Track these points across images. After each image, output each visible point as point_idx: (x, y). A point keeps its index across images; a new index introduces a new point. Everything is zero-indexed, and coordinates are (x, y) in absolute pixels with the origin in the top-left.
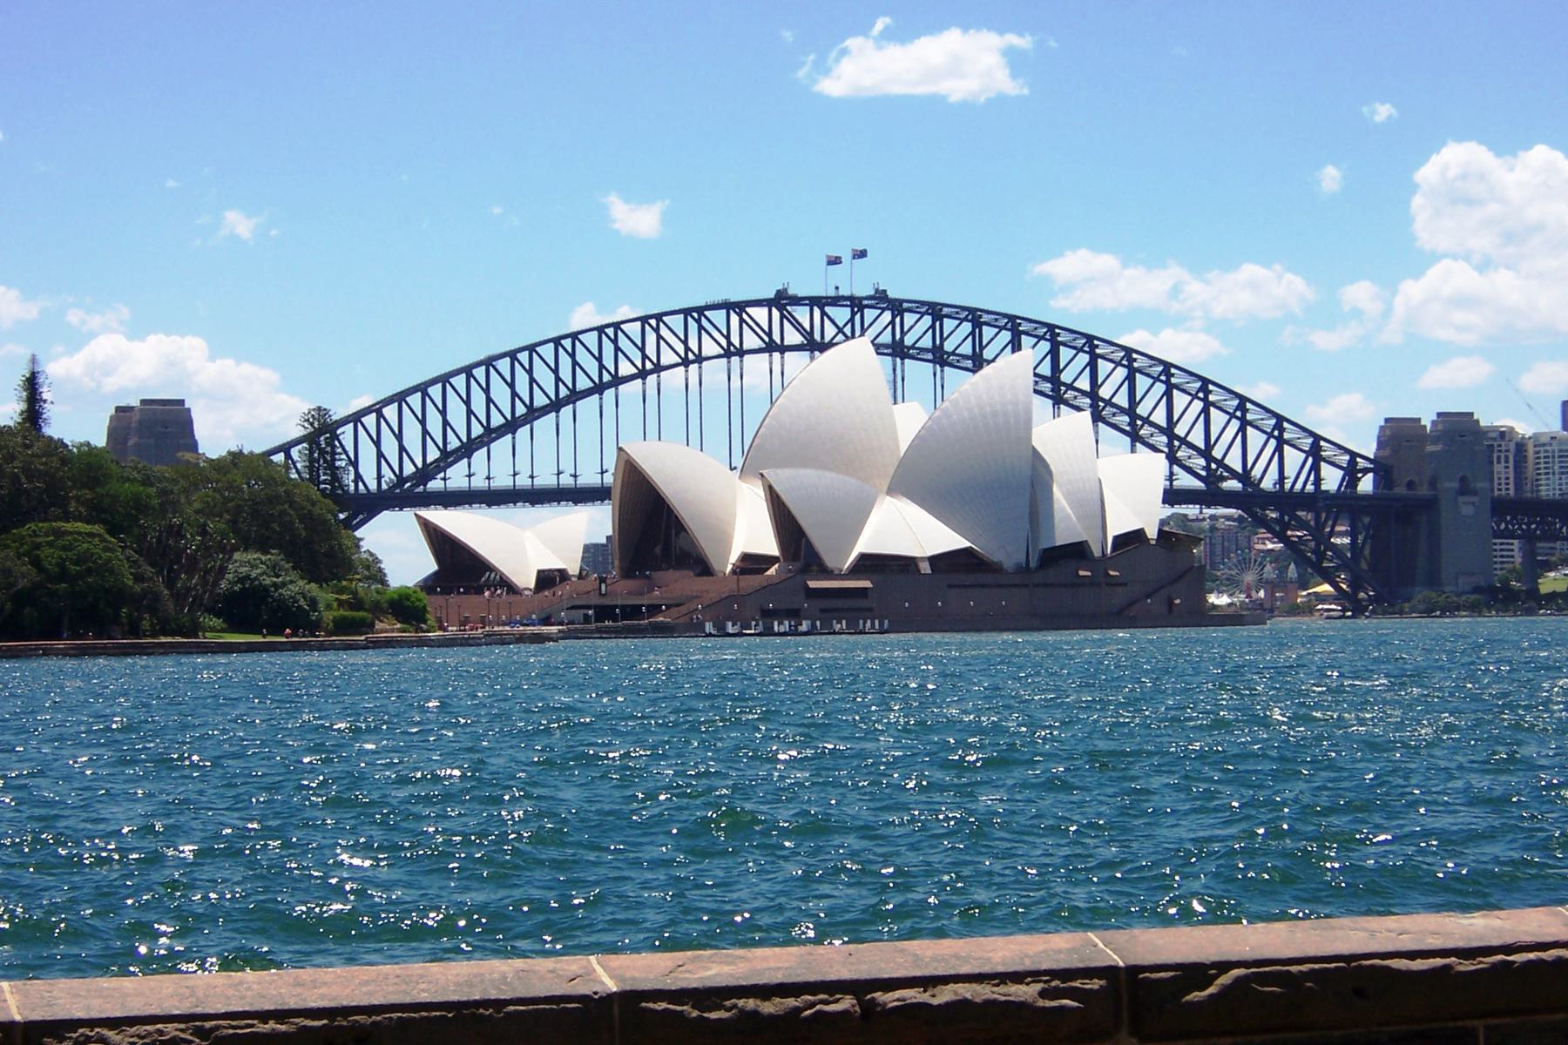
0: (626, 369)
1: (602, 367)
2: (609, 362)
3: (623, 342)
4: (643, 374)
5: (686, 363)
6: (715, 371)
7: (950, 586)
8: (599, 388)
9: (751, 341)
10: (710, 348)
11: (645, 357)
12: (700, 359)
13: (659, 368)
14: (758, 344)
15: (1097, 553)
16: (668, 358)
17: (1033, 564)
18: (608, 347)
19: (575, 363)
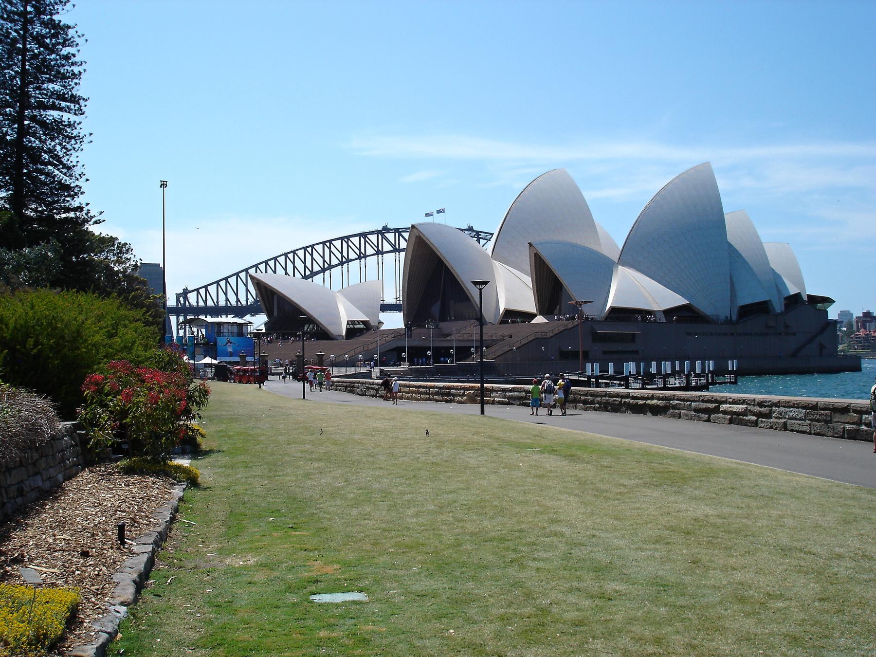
0: (335, 261)
1: (324, 261)
2: (327, 259)
3: (333, 248)
4: (341, 264)
5: (360, 258)
6: (372, 261)
7: (688, 334)
8: (323, 270)
9: (387, 247)
10: (370, 251)
11: (343, 256)
12: (365, 256)
13: (349, 261)
14: (391, 249)
15: (778, 310)
16: (352, 256)
17: (734, 318)
18: (327, 250)
19: (313, 259)
